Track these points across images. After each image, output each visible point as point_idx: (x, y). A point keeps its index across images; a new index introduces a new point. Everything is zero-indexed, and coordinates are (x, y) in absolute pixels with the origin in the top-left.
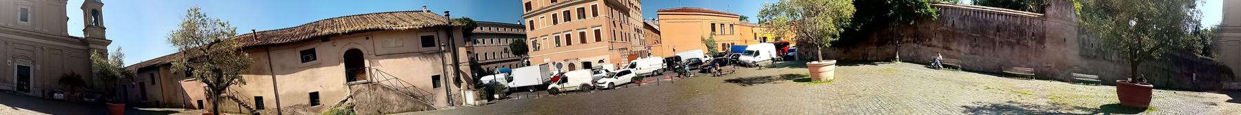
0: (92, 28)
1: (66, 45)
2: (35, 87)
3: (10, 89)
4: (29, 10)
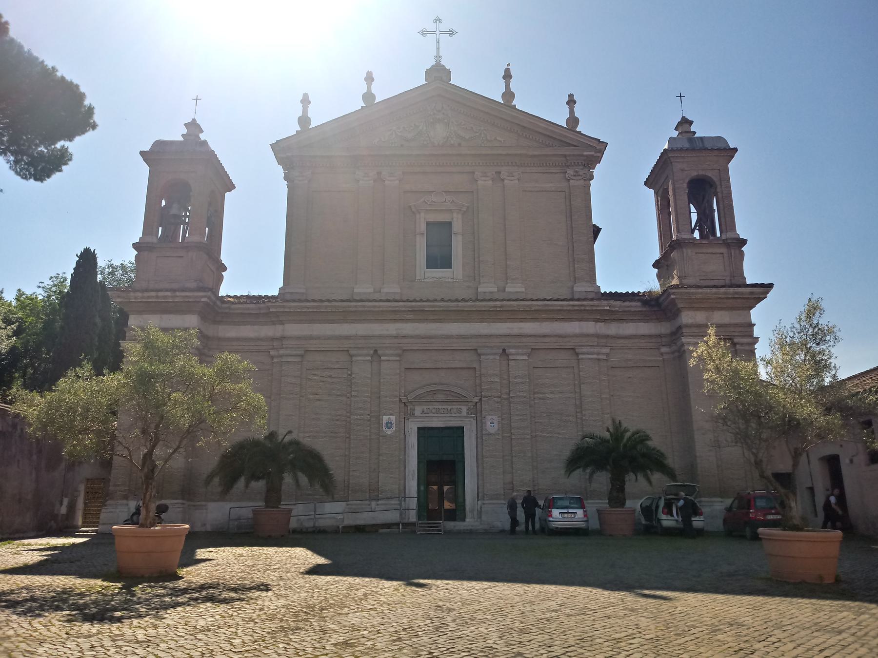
0: (688, 252)
1: (590, 327)
2: (480, 496)
3: (392, 517)
4: (457, 227)
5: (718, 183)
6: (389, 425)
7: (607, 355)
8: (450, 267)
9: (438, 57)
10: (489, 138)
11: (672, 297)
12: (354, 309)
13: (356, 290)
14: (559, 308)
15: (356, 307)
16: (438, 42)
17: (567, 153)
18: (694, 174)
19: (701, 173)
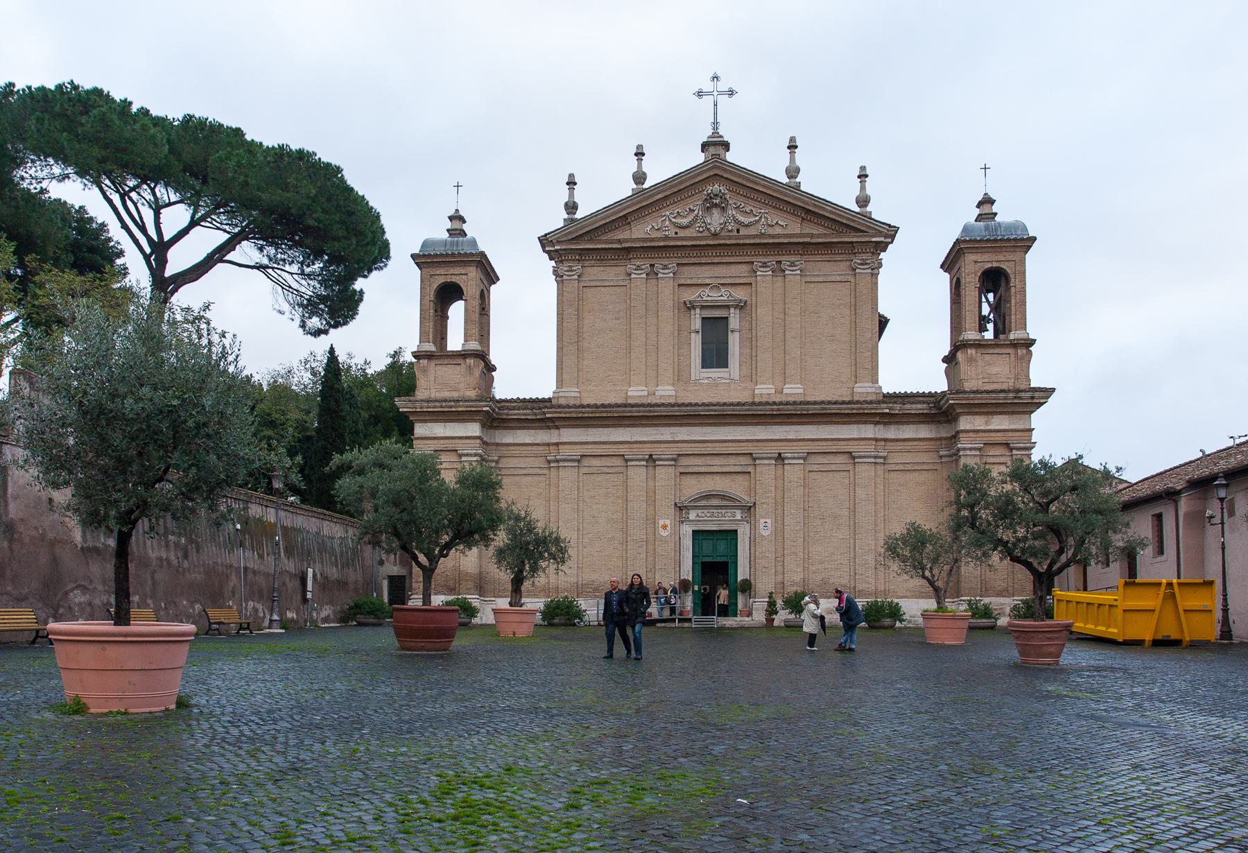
1: (869, 431)
4: (734, 323)
5: (1012, 276)
6: (665, 527)
7: (885, 458)
8: (727, 367)
9: (715, 124)
10: (770, 222)
11: (950, 402)
12: (629, 414)
13: (630, 393)
14: (837, 411)
15: (630, 412)
16: (716, 105)
17: (855, 240)
18: (989, 265)
19: (995, 265)
